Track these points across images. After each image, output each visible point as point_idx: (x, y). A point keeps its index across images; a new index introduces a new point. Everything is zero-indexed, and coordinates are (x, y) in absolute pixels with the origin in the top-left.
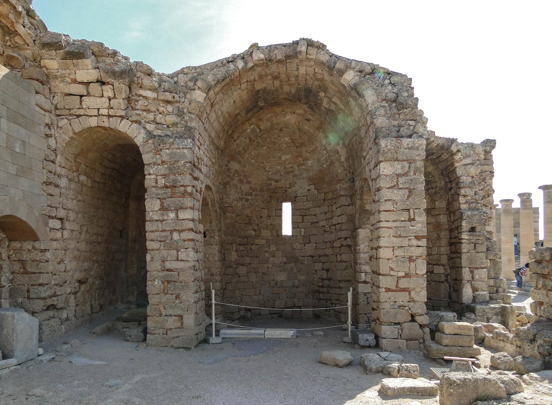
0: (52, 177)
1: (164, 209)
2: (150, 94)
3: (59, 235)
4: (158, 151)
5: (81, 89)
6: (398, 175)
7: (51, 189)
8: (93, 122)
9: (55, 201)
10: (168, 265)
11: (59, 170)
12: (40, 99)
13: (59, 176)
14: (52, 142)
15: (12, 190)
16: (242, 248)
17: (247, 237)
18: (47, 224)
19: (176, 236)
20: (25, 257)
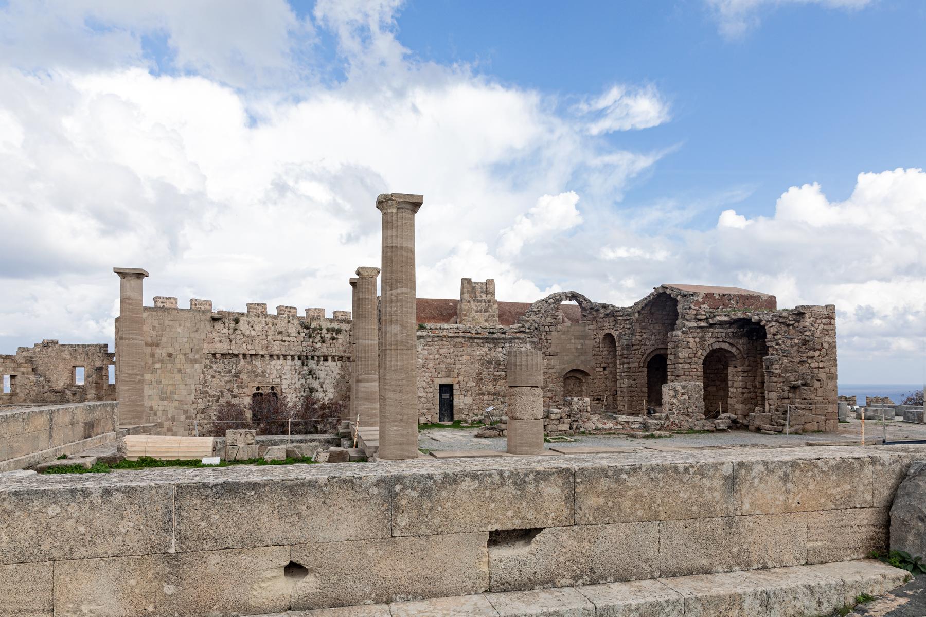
0: (596, 353)
1: (620, 364)
2: (620, 318)
3: (602, 373)
4: (619, 342)
5: (601, 320)
6: (673, 348)
7: (596, 357)
8: (607, 331)
9: (599, 361)
10: (622, 386)
11: (601, 349)
12: (591, 327)
13: (603, 351)
14: (598, 340)
15: (576, 361)
16: (712, 376)
17: (718, 369)
18: (595, 370)
19: (623, 374)
20: (589, 381)
